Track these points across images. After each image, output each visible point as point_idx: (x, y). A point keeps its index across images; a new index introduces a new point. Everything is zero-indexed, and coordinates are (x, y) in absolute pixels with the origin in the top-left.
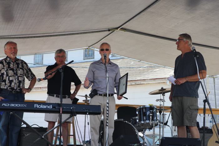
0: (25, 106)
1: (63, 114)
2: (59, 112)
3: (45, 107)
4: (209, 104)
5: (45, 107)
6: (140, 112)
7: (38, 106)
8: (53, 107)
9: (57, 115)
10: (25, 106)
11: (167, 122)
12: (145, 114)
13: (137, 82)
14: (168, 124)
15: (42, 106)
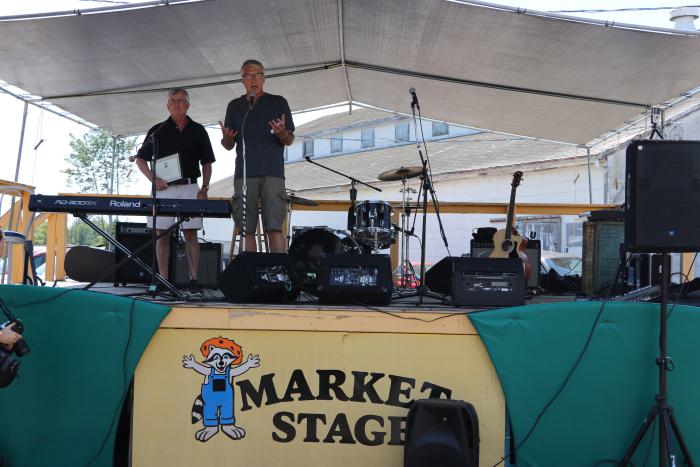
0: (94, 203)
1: (159, 219)
2: (147, 213)
3: (128, 205)
4: (432, 192)
5: (128, 205)
6: (359, 213)
7: (116, 204)
8: (143, 205)
9: (152, 218)
10: (94, 203)
11: (413, 229)
12: (366, 214)
13: (547, 166)
14: (415, 233)
15: (123, 204)
